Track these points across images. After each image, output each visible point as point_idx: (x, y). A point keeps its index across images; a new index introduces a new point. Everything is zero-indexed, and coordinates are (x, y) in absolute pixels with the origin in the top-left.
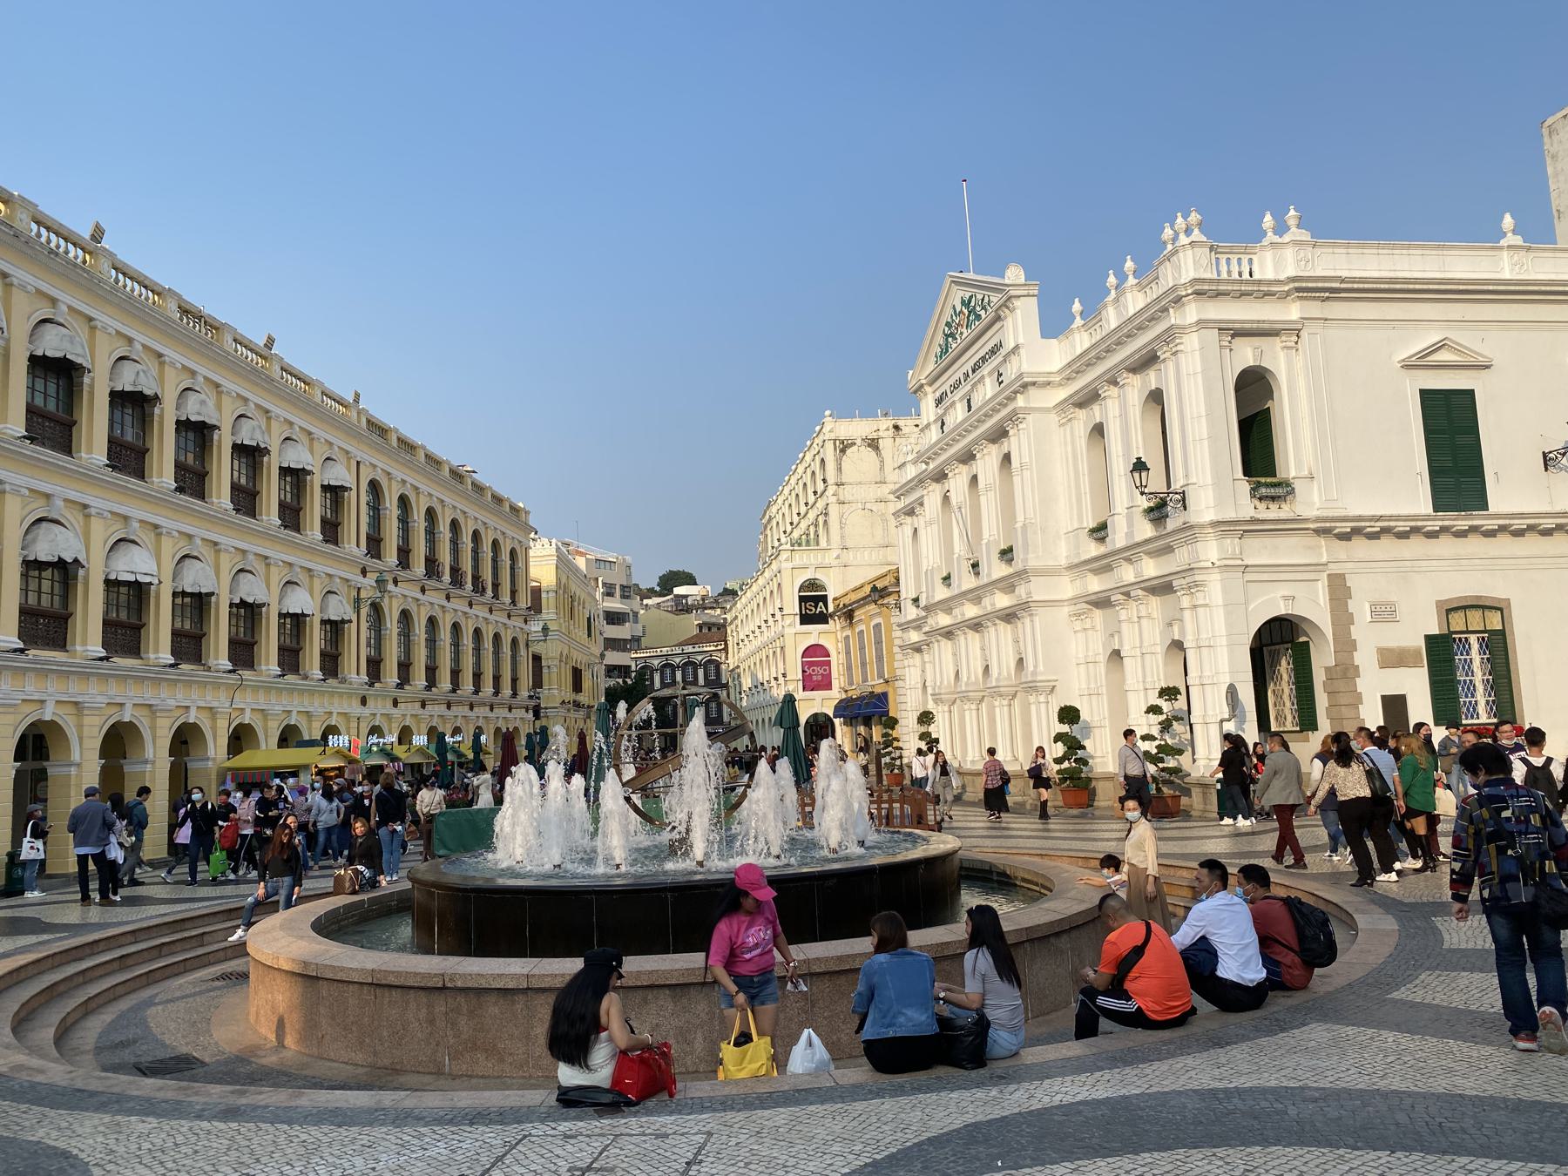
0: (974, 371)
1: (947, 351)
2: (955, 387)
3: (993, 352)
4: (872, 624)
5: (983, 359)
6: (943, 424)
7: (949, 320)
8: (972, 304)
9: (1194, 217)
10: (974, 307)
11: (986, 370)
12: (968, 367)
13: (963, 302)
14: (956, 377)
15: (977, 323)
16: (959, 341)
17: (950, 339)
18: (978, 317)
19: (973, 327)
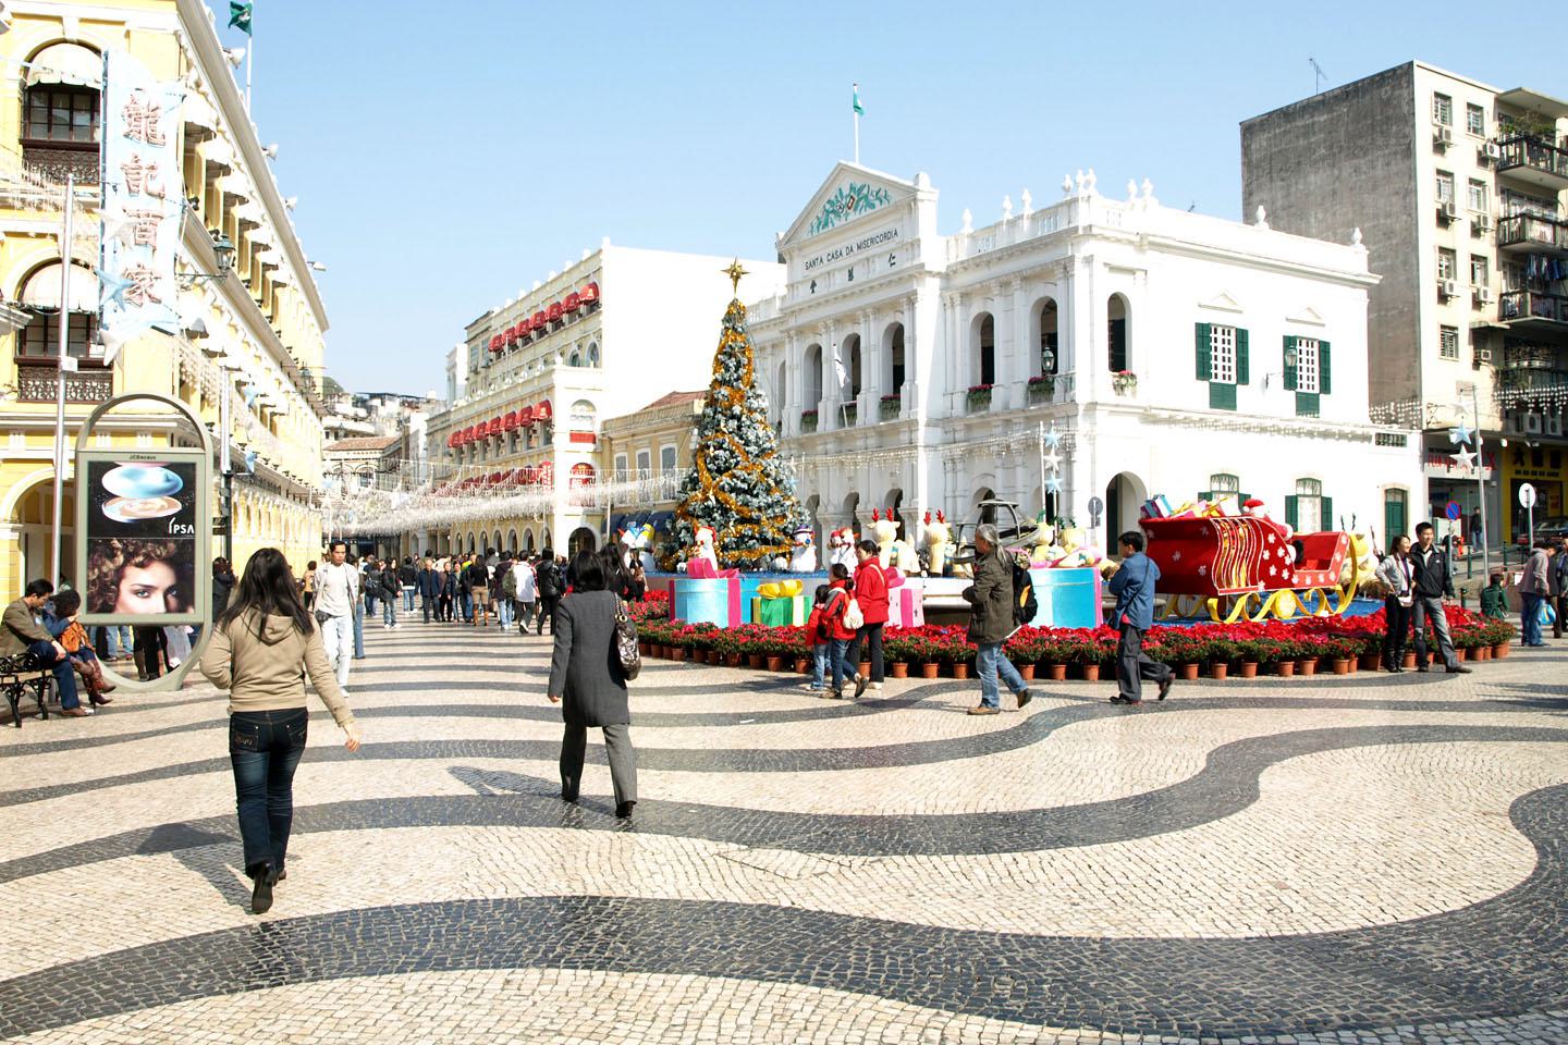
0: (859, 247)
1: (826, 225)
2: (835, 256)
3: (886, 236)
4: (662, 448)
5: (872, 240)
6: (814, 285)
7: (833, 198)
8: (865, 191)
9: (1092, 177)
10: (866, 197)
11: (873, 250)
12: (854, 243)
13: (852, 188)
14: (838, 247)
15: (869, 211)
16: (843, 222)
17: (832, 216)
18: (873, 206)
19: (863, 213)
